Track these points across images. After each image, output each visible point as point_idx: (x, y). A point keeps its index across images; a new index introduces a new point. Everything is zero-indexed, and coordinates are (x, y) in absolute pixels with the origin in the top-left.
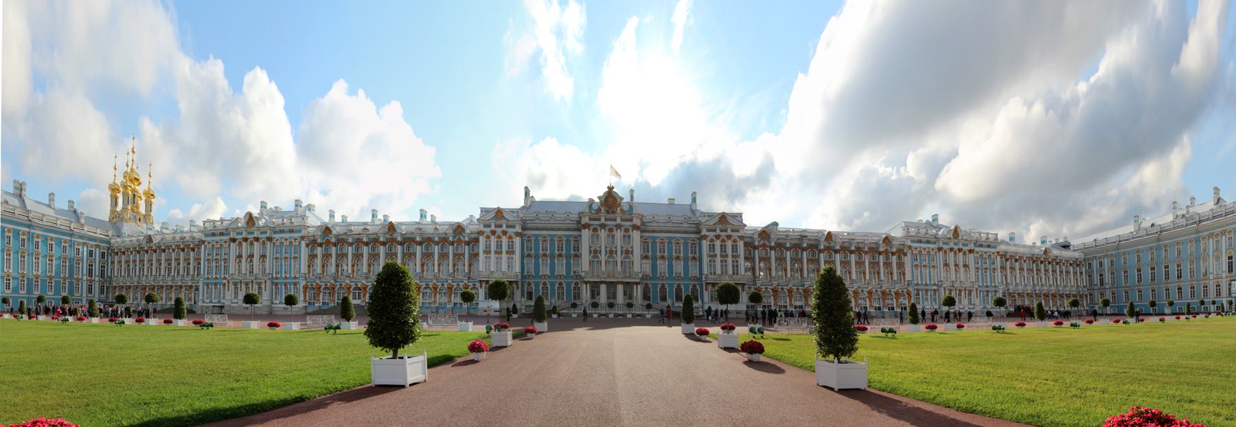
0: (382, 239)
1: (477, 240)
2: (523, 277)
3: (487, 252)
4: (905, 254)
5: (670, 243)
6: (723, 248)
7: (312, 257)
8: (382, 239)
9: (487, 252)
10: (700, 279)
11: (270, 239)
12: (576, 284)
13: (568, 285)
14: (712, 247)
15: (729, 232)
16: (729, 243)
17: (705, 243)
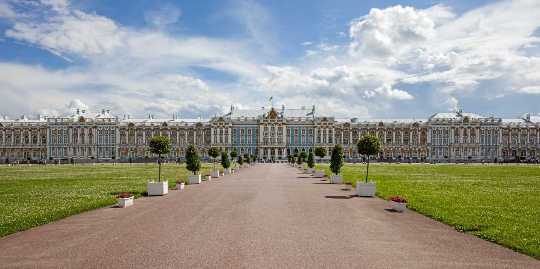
0: (161, 129)
1: (210, 130)
2: (233, 145)
3: (215, 133)
4: (428, 131)
5: (300, 129)
6: (325, 131)
7: (123, 135)
8: (161, 129)
9: (215, 133)
10: (313, 145)
11: (95, 127)
12: (257, 148)
13: (253, 148)
14: (319, 132)
15: (327, 125)
16: (327, 130)
17: (316, 130)
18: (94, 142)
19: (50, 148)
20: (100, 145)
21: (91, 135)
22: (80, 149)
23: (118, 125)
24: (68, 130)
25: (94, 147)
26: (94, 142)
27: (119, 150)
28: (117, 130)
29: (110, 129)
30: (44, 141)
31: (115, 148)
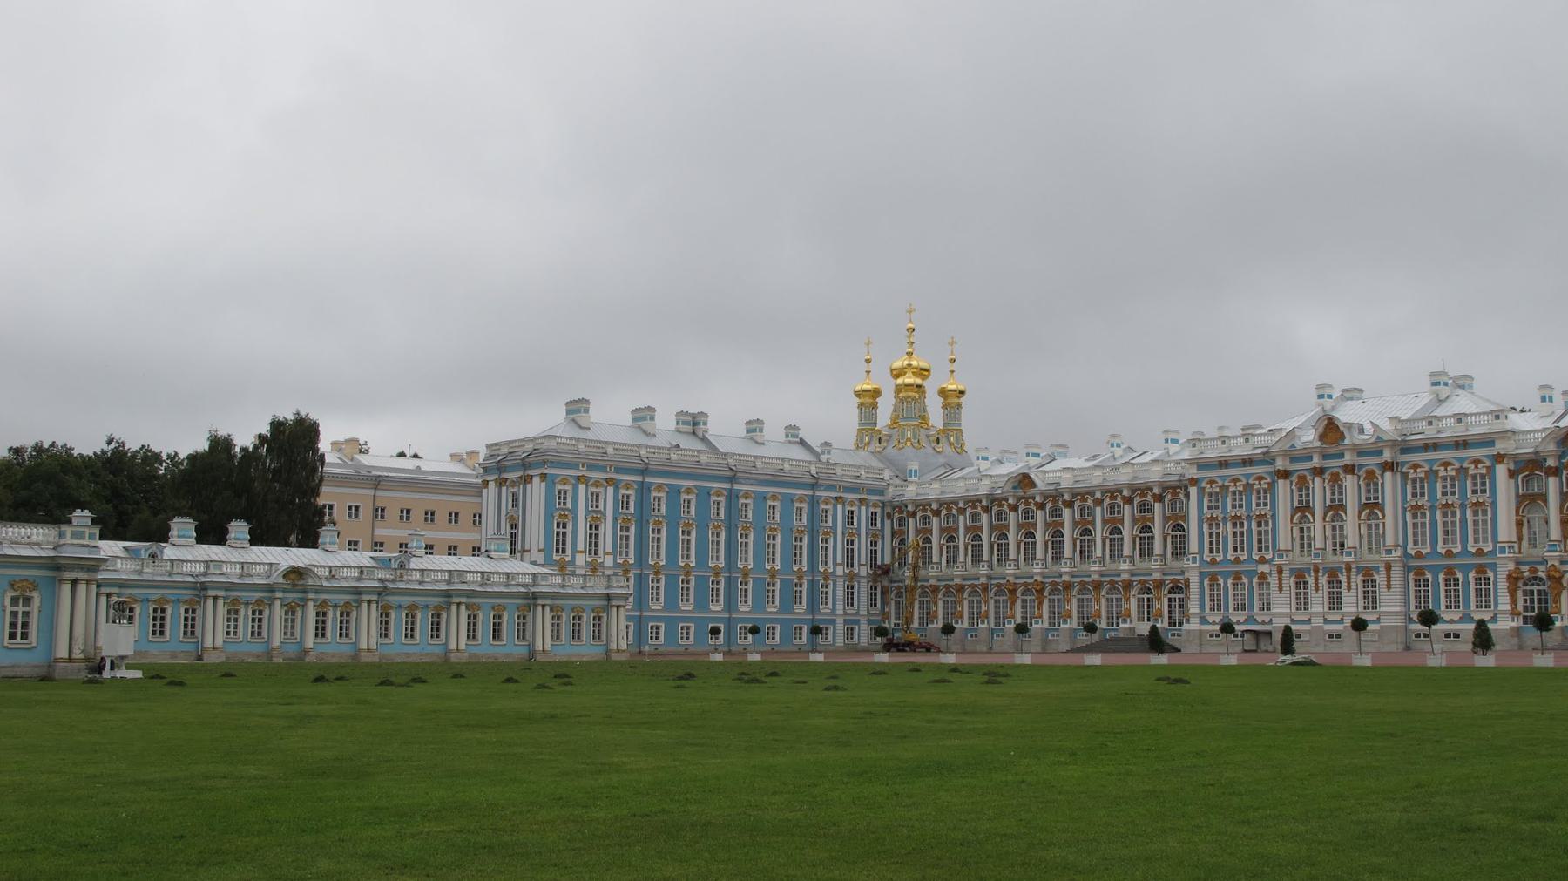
7: (1529, 501)
11: (1389, 467)
18: (1390, 541)
19: (1202, 575)
20: (1419, 555)
21: (1372, 507)
22: (1323, 580)
23: (1500, 447)
24: (1272, 485)
25: (1388, 567)
26: (1390, 541)
27: (1513, 579)
28: (1501, 471)
29: (1462, 471)
30: (1179, 551)
31: (1493, 567)
